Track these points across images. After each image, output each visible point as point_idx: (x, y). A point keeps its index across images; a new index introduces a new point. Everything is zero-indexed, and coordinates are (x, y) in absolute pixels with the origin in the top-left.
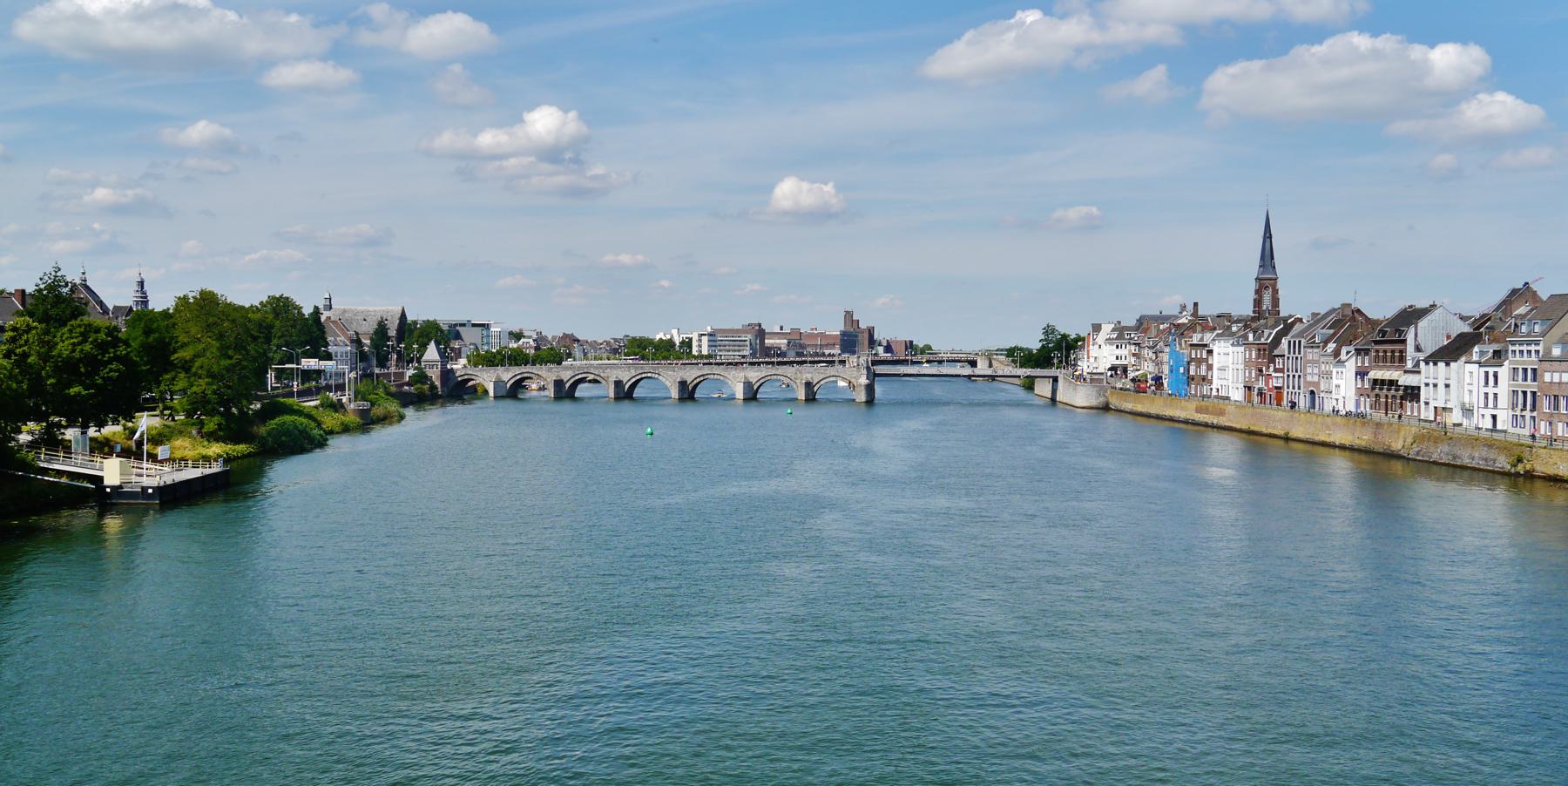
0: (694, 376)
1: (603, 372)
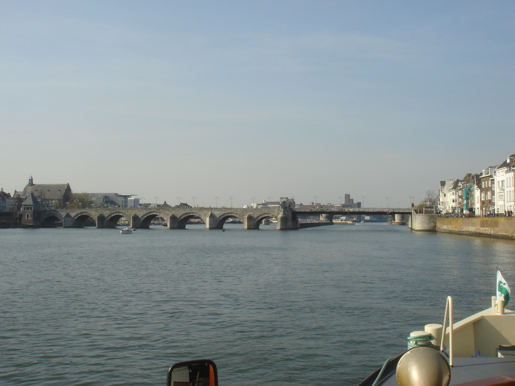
0: (181, 214)
1: (128, 212)
